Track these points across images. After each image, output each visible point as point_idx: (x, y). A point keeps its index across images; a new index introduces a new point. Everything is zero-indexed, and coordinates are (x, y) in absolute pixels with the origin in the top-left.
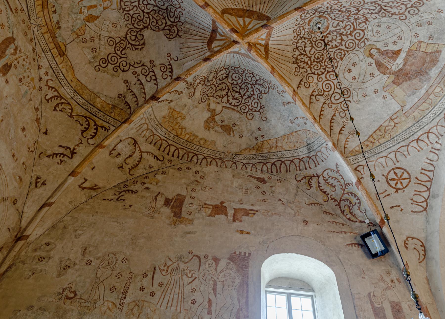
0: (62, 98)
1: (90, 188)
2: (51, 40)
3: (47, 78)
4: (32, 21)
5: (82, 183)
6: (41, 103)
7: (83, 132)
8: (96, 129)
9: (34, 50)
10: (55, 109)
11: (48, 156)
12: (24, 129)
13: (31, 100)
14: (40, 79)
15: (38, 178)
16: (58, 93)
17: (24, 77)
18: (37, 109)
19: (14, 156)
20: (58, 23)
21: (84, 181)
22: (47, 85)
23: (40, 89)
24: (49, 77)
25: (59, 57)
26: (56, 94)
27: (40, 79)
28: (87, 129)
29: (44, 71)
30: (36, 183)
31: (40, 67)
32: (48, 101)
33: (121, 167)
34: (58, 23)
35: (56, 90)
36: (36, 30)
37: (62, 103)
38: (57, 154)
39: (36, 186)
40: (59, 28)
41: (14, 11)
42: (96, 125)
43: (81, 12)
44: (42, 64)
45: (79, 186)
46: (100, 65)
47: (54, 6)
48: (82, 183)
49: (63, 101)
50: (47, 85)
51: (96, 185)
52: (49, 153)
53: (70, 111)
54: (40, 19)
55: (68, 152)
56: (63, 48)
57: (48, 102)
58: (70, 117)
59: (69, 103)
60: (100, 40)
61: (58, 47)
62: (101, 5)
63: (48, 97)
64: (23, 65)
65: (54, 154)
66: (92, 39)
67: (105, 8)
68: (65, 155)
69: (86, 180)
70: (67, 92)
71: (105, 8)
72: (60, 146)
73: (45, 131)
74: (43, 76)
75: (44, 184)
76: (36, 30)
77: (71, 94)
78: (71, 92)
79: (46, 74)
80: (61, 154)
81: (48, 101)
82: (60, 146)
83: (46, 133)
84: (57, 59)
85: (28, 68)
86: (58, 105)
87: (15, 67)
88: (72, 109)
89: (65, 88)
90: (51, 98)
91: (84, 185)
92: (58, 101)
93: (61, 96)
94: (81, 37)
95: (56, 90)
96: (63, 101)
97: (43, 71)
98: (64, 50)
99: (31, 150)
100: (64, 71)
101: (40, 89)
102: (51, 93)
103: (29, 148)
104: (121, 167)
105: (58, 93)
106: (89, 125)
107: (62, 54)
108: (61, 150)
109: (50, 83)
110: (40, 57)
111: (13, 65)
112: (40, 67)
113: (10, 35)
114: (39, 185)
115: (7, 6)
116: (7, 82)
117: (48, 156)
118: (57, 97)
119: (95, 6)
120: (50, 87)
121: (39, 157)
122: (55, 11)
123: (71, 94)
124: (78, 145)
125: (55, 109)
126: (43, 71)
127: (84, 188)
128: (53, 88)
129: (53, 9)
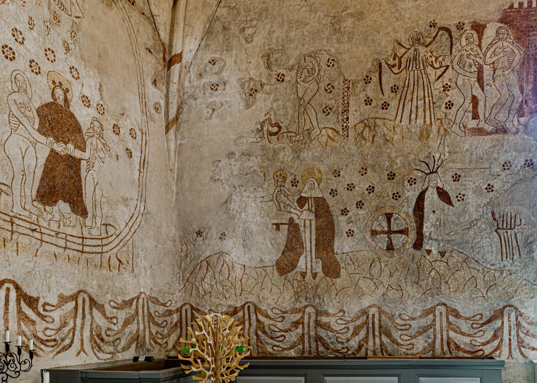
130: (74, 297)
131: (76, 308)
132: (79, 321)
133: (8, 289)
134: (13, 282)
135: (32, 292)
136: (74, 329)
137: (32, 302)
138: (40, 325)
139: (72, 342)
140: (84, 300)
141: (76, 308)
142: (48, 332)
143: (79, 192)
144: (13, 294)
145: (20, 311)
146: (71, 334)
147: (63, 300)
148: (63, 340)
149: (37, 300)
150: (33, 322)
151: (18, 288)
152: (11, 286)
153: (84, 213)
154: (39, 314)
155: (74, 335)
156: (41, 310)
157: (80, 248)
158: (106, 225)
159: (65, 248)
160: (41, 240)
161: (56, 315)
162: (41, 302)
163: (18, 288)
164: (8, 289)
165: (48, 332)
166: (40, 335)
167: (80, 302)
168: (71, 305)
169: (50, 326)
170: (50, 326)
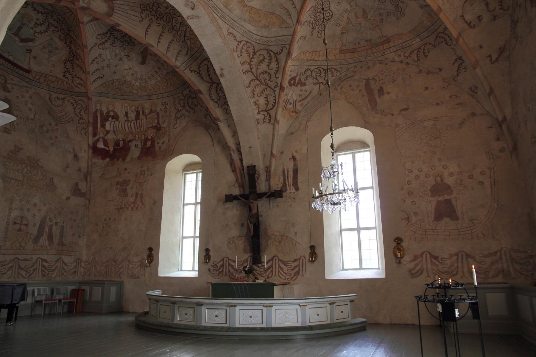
0: (420, 48)
1: (500, 55)
2: (377, 48)
3: (402, 56)
4: (364, 60)
5: (491, 60)
6: (418, 66)
7: (447, 44)
8: (446, 34)
9: (381, 63)
10: (426, 56)
11: (458, 75)
12: (426, 88)
13: (410, 76)
14: (401, 62)
15: (471, 89)
16: (416, 50)
17: (393, 77)
18: (420, 71)
19: (437, 104)
20: (367, 41)
21: (489, 58)
22: (407, 57)
23: (407, 64)
24: (402, 54)
25: (390, 43)
26: (416, 52)
27: (401, 62)
28: (445, 40)
29: (397, 57)
30: (473, 91)
31: (393, 61)
32: (418, 60)
33: (495, 18)
34: (367, 41)
35: (413, 51)
36: (369, 58)
37: (424, 49)
38: (458, 69)
39: (476, 93)
40: (370, 40)
41: (354, 74)
42: (443, 33)
43: (360, 24)
44: (391, 58)
45: (492, 63)
46: (400, 12)
47: (355, 44)
48: (491, 60)
49: (422, 48)
50: (407, 57)
51: (500, 48)
52: (455, 74)
53: (431, 46)
54: (363, 54)
55: (459, 62)
56: (384, 39)
57: (419, 60)
58: (435, 47)
59: (425, 44)
60: (381, 9)
61: (383, 43)
62: (354, 9)
63: (416, 59)
64: (386, 76)
65: (457, 71)
66: (381, 15)
67: (357, 5)
68: (461, 64)
69: (490, 56)
70: (417, 43)
71: (357, 5)
72: (453, 64)
73: (439, 70)
74: (400, 59)
75: (476, 88)
76: (369, 58)
77: (419, 40)
78: (418, 40)
79: (399, 56)
80: (459, 66)
81: (418, 60)
82: (453, 64)
83: (441, 70)
84: (391, 46)
85: (389, 72)
86: (424, 53)
87: (383, 83)
88: (430, 44)
89: (413, 43)
90: (417, 57)
91: (494, 58)
92: (422, 51)
93: (418, 49)
94: (378, 23)
95: (413, 51)
96: (422, 48)
97: (397, 59)
98: (386, 38)
99: (446, 87)
100: (401, 41)
101: (407, 64)
102: (414, 56)
103: (444, 87)
104: (495, 18)
105: (416, 50)
106: (443, 38)
107: (388, 41)
108: (457, 65)
109: (407, 54)
110: (386, 59)
111: (381, 85)
112: (393, 61)
113: (365, 81)
114: (476, 91)
115: (350, 79)
116: (388, 93)
117: (458, 75)
118: (418, 51)
119: (356, 13)
120: (409, 56)
121: (456, 81)
122: (359, 43)
123: (419, 40)
124: (456, 53)
125: (426, 56)
126: (397, 59)
127: (497, 60)
128: (411, 53)
129: (357, 44)
130: (457, 254)
131: (458, 259)
132: (460, 264)
133: (426, 254)
134: (428, 252)
135: (435, 254)
136: (458, 267)
137: (436, 258)
138: (440, 267)
139: (457, 273)
140: (462, 256)
141: (458, 259)
142: (444, 269)
143: (454, 211)
144: (428, 256)
145: (432, 261)
146: (456, 270)
147: (451, 256)
148: (452, 272)
149: (438, 257)
150: (437, 265)
151: (430, 253)
152: (427, 253)
153: (457, 219)
154: (440, 262)
155: (458, 270)
156: (440, 261)
157: (458, 233)
158: (472, 220)
159: (450, 235)
160: (438, 235)
161: (448, 262)
162: (440, 257)
163: (430, 253)
164: (426, 254)
165: (444, 269)
166: (441, 270)
167: (460, 256)
168: (455, 258)
169: (445, 266)
170: (445, 266)
